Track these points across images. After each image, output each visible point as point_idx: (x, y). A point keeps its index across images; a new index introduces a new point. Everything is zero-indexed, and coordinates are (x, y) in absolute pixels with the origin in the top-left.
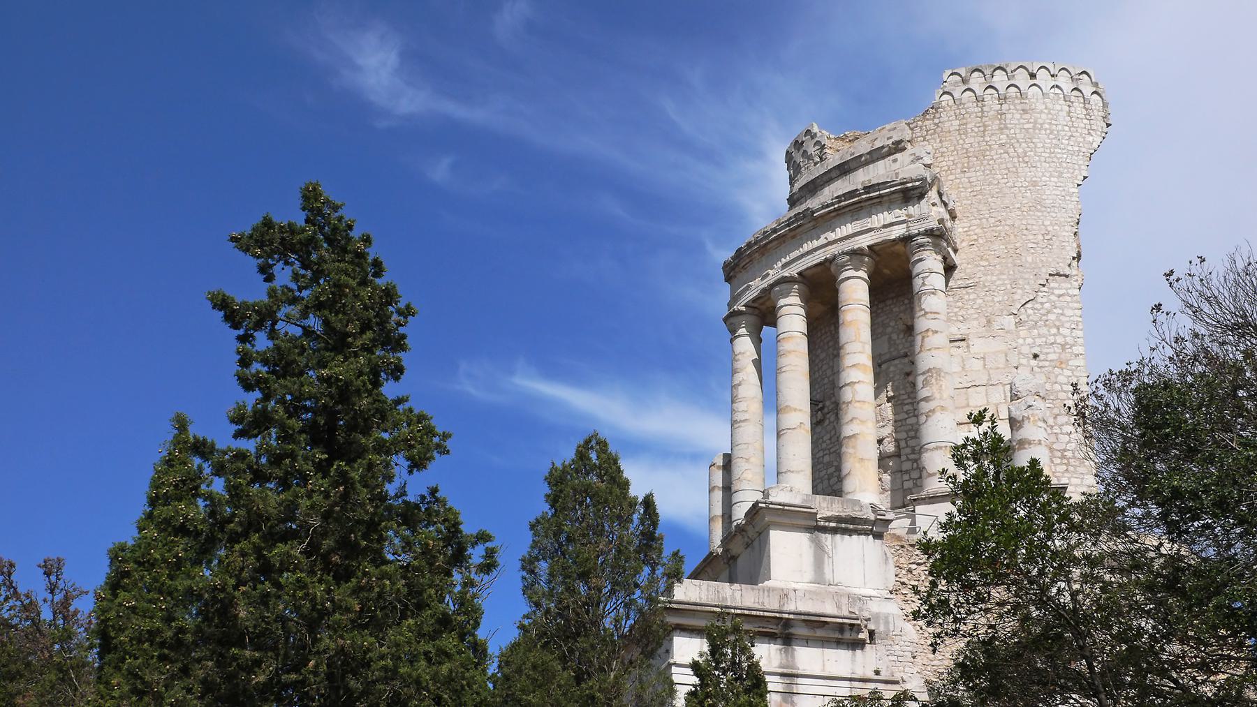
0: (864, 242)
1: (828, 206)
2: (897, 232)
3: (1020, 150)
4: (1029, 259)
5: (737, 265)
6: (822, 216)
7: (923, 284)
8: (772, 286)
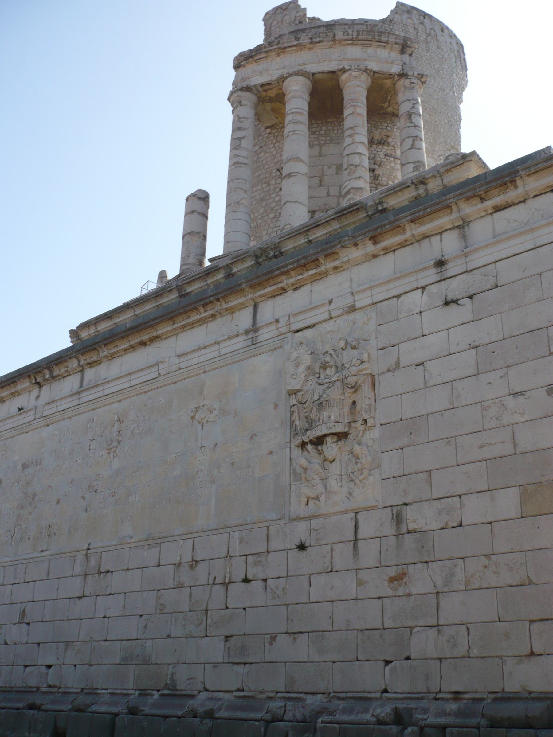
0: (374, 66)
1: (348, 34)
2: (395, 69)
3: (436, 67)
4: (442, 130)
5: (251, 57)
6: (340, 41)
7: (413, 107)
8: (290, 75)
